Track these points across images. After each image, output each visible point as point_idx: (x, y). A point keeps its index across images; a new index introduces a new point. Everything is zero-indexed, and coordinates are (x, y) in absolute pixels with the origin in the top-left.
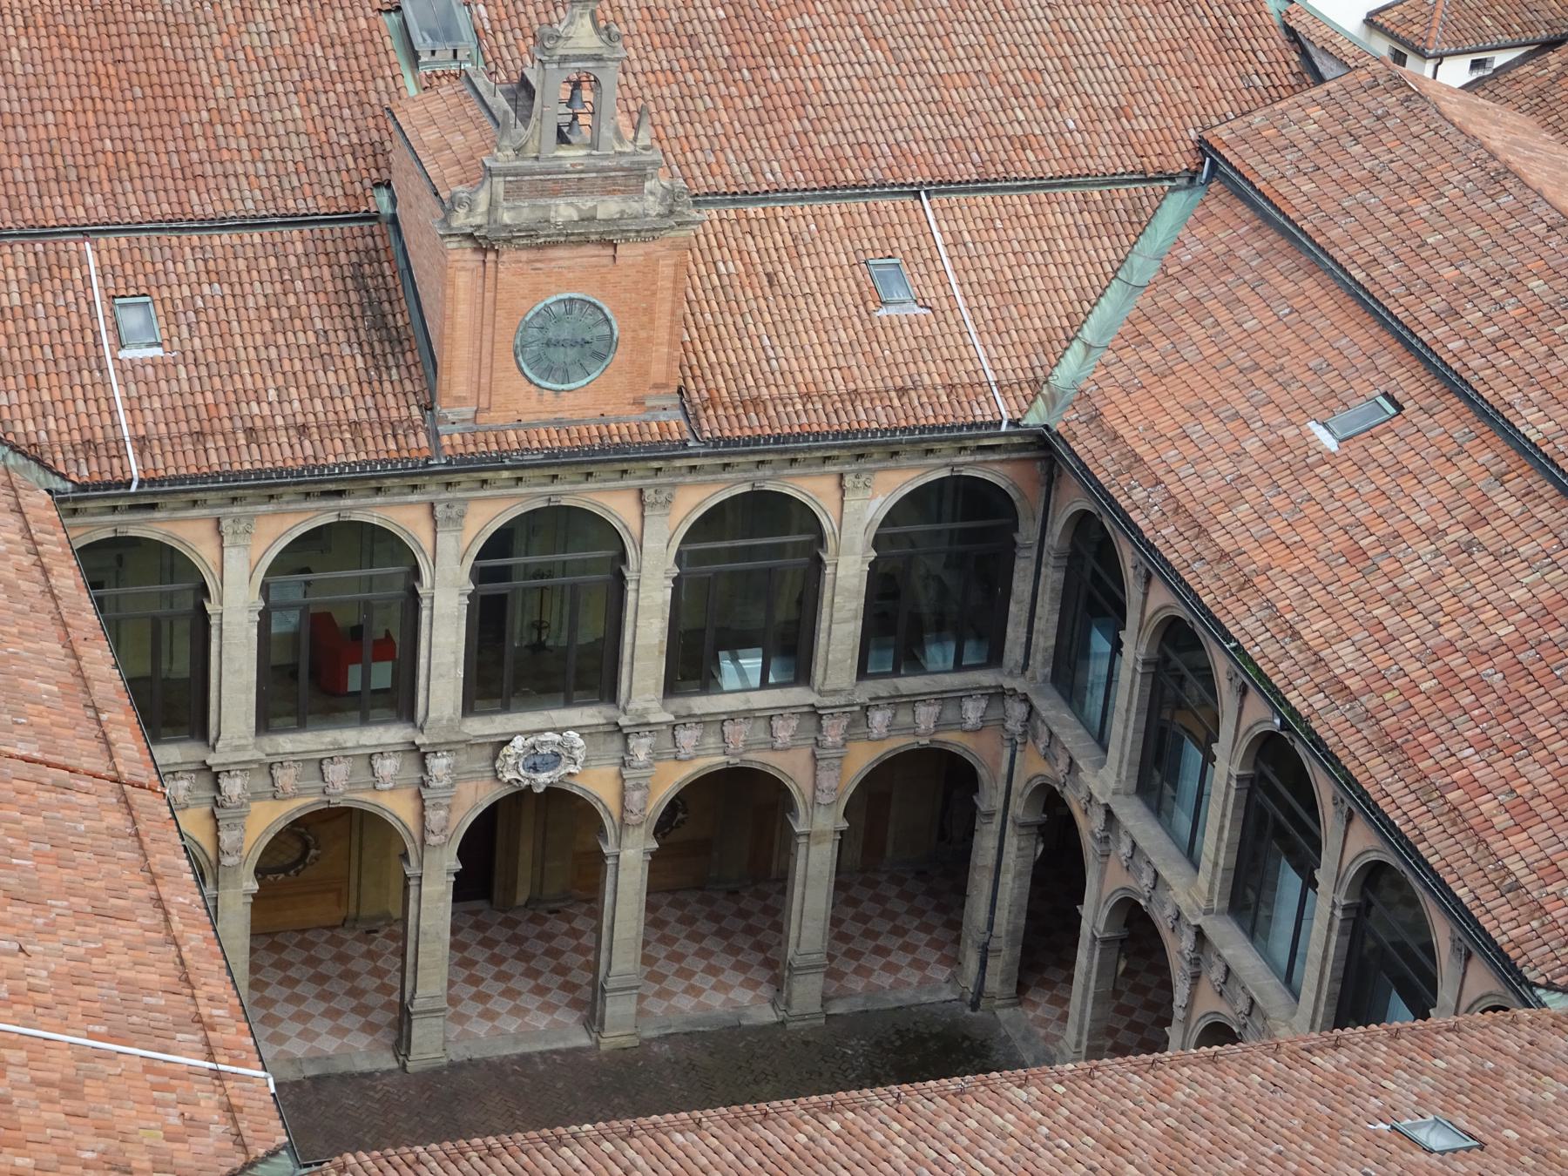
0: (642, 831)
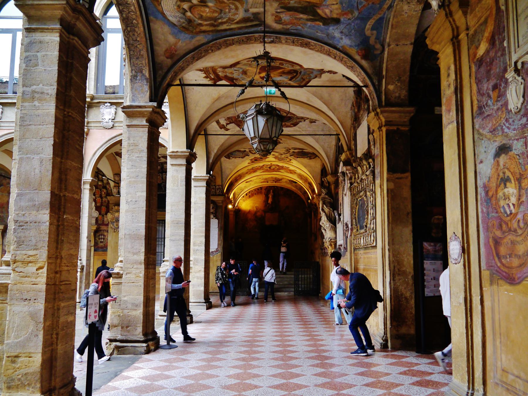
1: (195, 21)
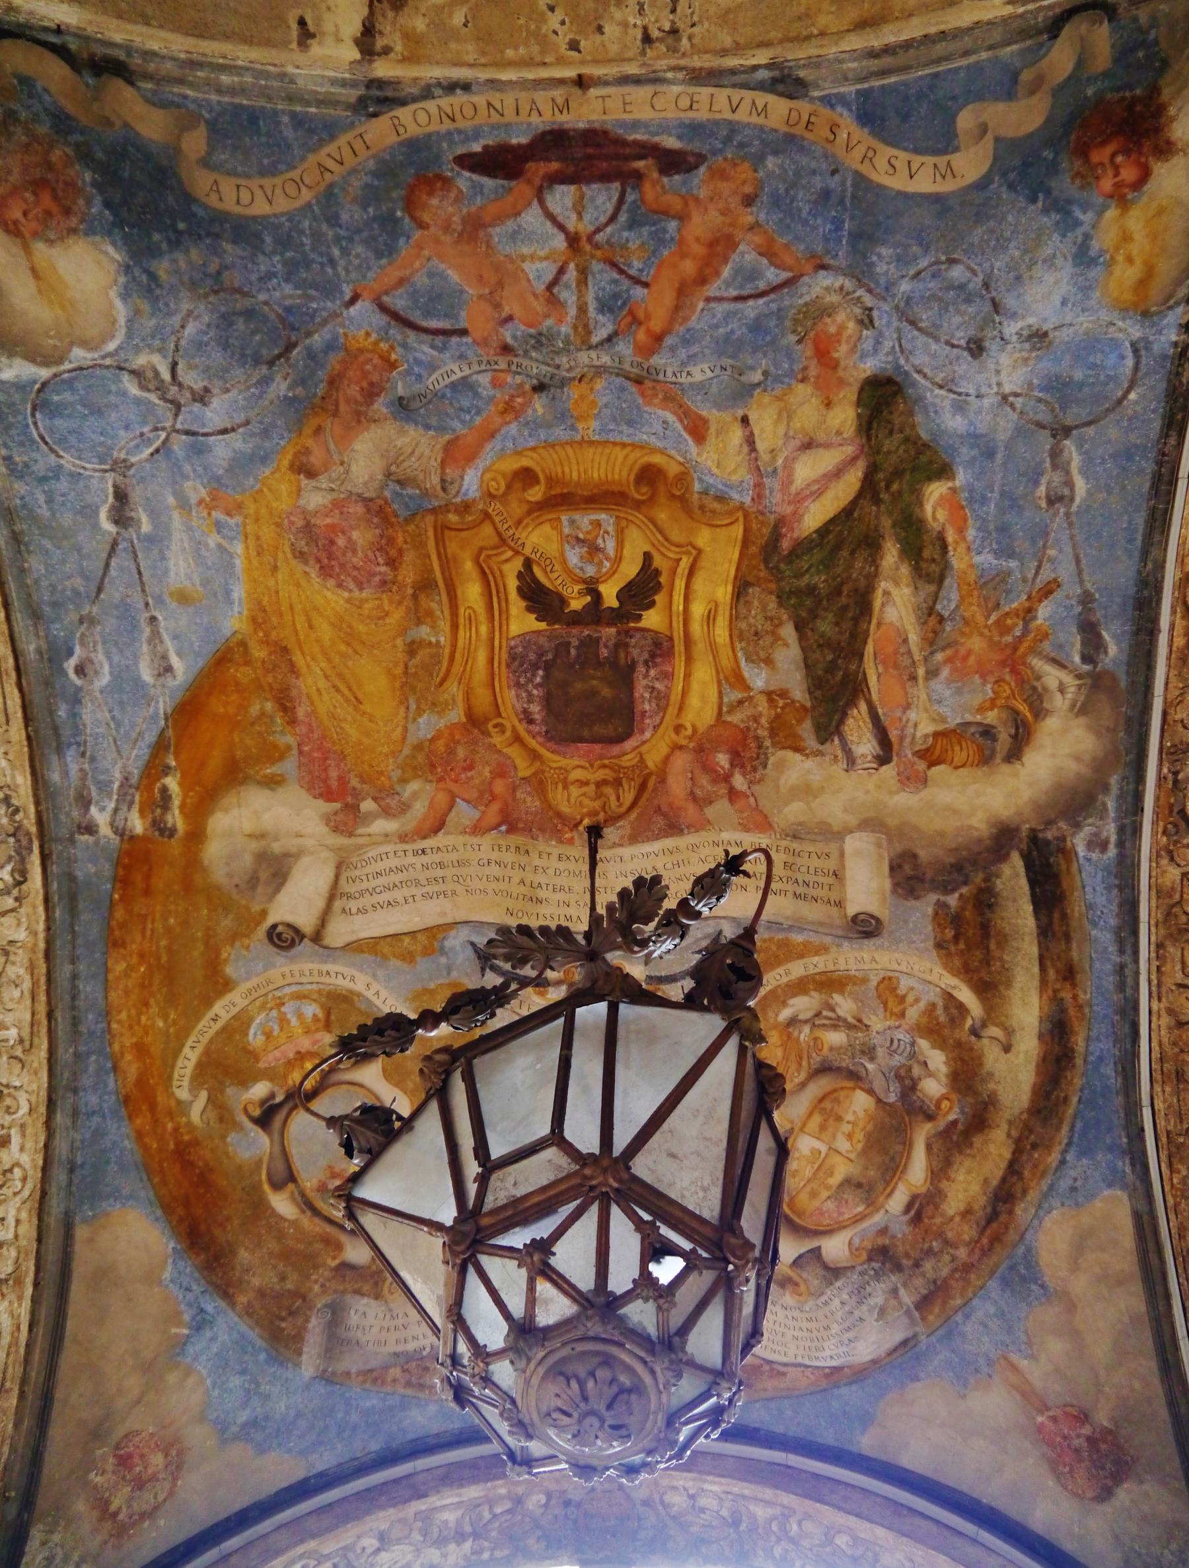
1: (883, 1231)
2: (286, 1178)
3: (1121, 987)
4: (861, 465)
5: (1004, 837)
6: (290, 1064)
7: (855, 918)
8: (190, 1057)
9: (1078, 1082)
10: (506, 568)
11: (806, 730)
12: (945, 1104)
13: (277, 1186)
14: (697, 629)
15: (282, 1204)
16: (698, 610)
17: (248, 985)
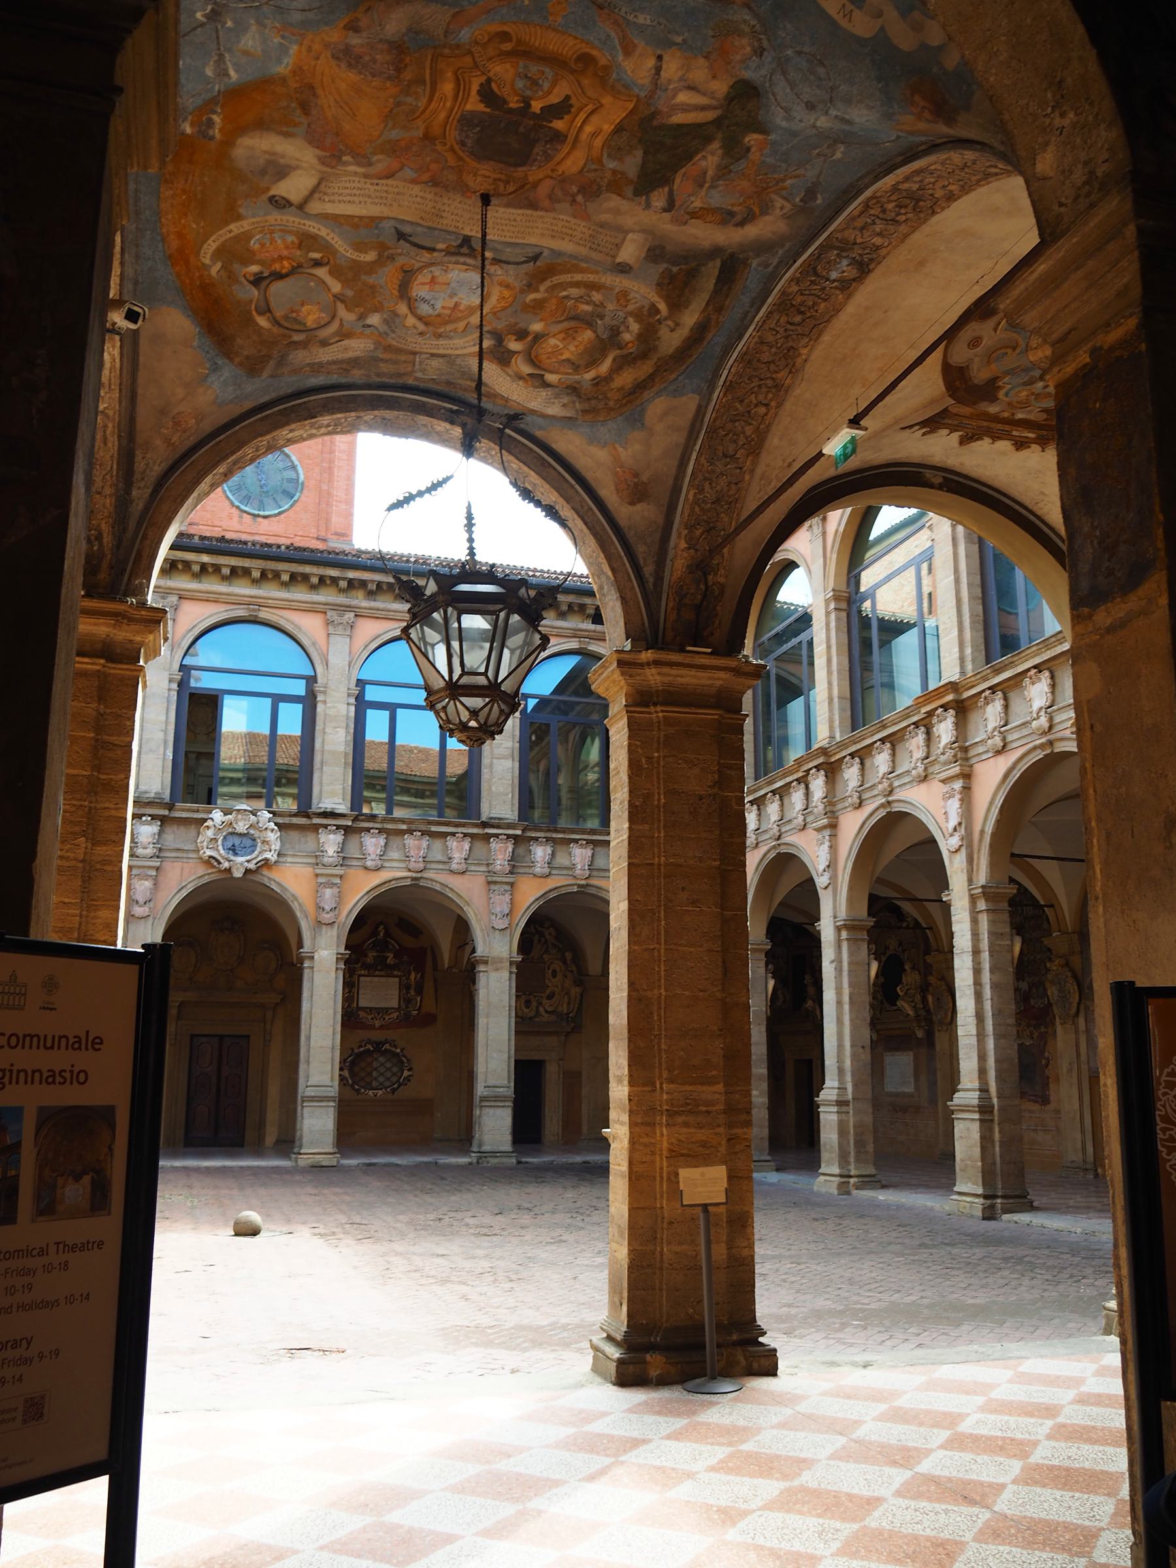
0: (333, 932)
1: (578, 383)
2: (266, 310)
3: (743, 320)
4: (718, 113)
5: (716, 251)
6: (274, 260)
7: (619, 264)
8: (212, 245)
9: (700, 350)
10: (473, 79)
11: (629, 191)
12: (630, 345)
13: (260, 313)
14: (583, 137)
15: (263, 322)
16: (588, 129)
17: (254, 220)
